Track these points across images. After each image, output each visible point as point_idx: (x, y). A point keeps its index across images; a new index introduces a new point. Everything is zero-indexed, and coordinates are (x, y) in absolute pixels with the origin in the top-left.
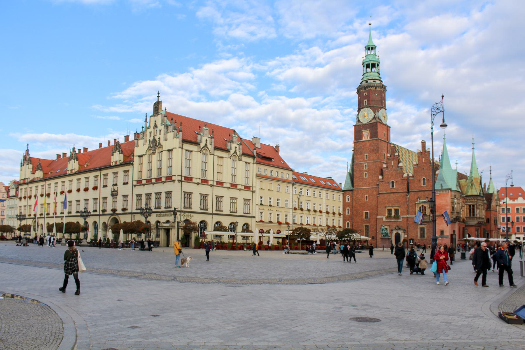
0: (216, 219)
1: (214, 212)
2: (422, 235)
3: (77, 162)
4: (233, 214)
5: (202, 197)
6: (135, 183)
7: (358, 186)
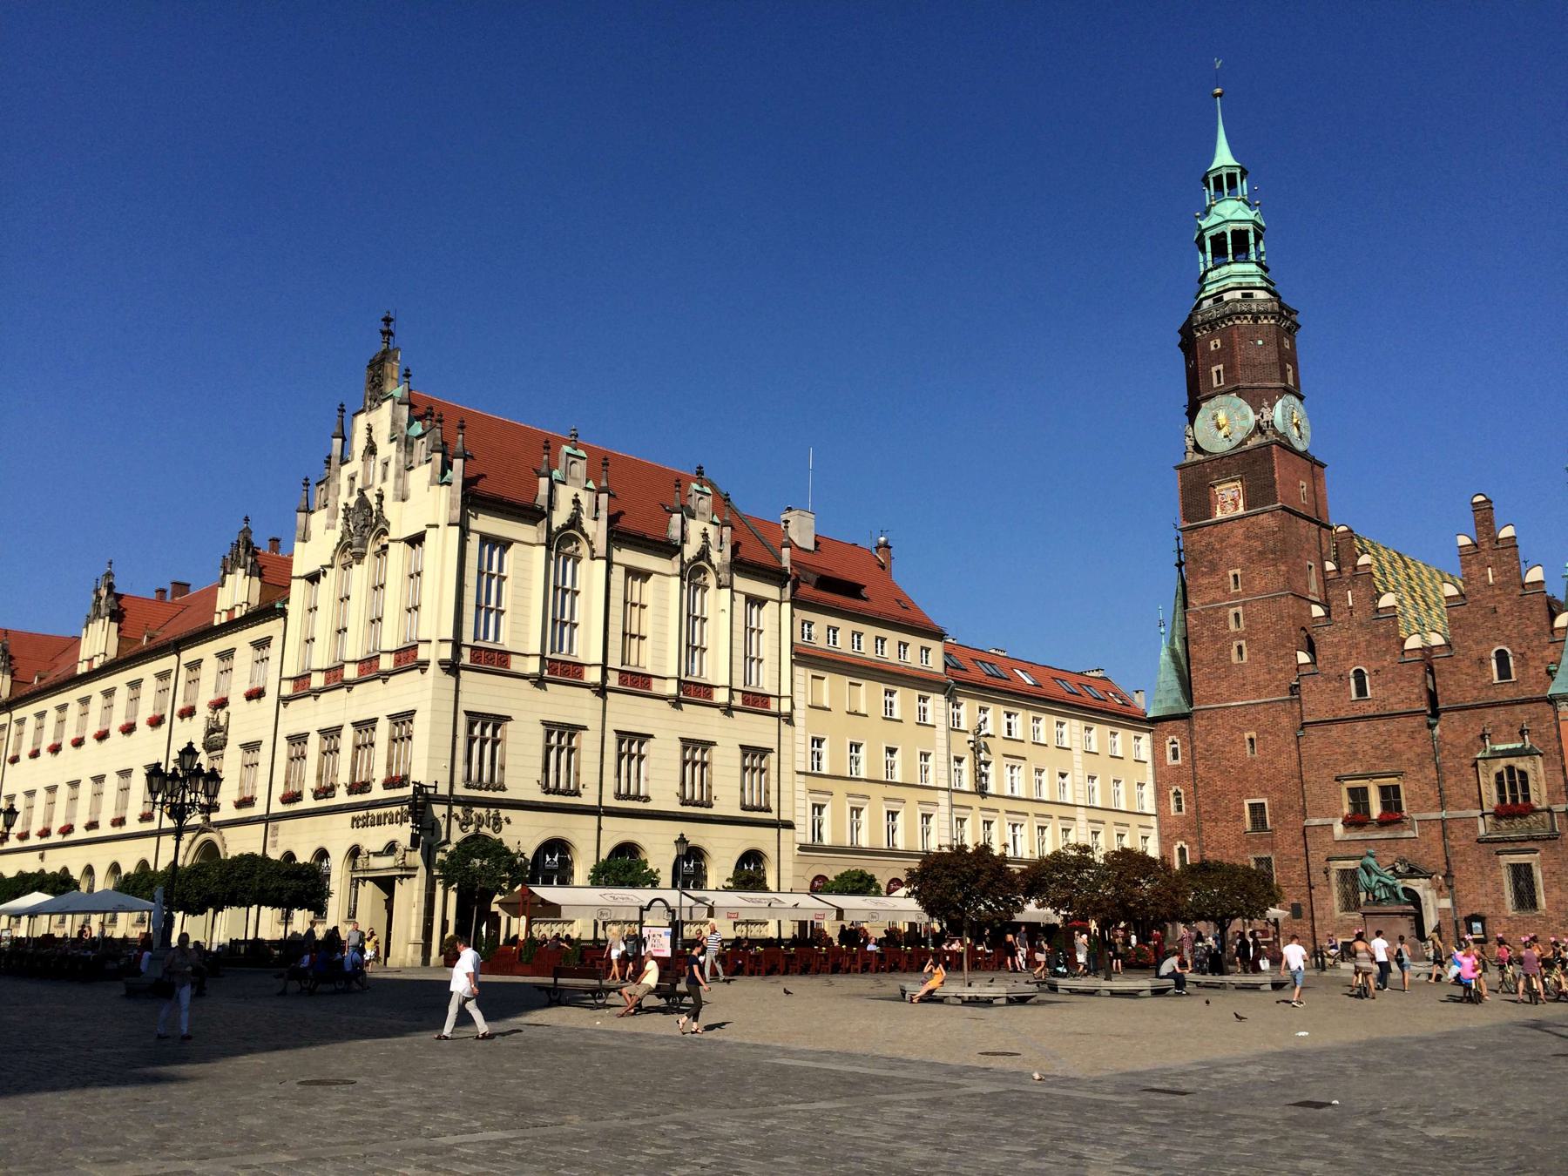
0: (617, 831)
1: (610, 801)
2: (1525, 898)
3: (114, 626)
4: (695, 809)
5: (554, 739)
6: (287, 689)
7: (1210, 698)
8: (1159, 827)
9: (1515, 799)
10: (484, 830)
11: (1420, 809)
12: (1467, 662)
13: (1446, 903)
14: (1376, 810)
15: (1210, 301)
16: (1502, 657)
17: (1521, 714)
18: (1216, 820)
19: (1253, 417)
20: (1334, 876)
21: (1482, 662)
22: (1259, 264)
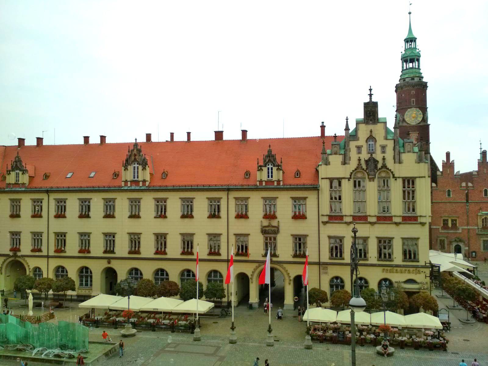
6: (326, 219)
11: (462, 226)
13: (467, 248)
14: (450, 225)
16: (486, 191)
21: (481, 191)
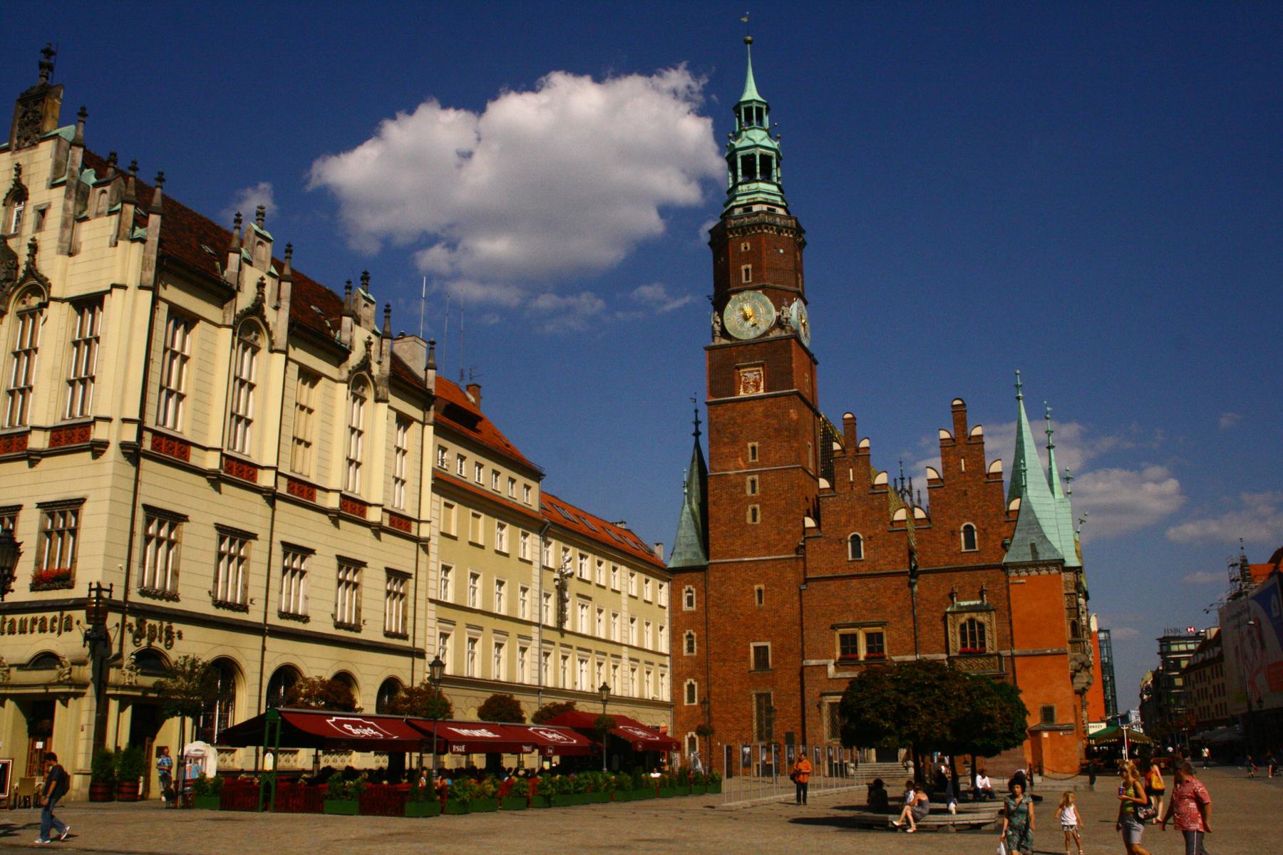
0: (281, 652)
1: (274, 620)
7: (724, 555)
8: (672, 666)
9: (973, 645)
10: (157, 644)
12: (942, 534)
14: (862, 653)
15: (741, 210)
16: (969, 530)
17: (983, 578)
18: (724, 660)
19: (775, 314)
20: (825, 709)
21: (954, 534)
22: (779, 186)
